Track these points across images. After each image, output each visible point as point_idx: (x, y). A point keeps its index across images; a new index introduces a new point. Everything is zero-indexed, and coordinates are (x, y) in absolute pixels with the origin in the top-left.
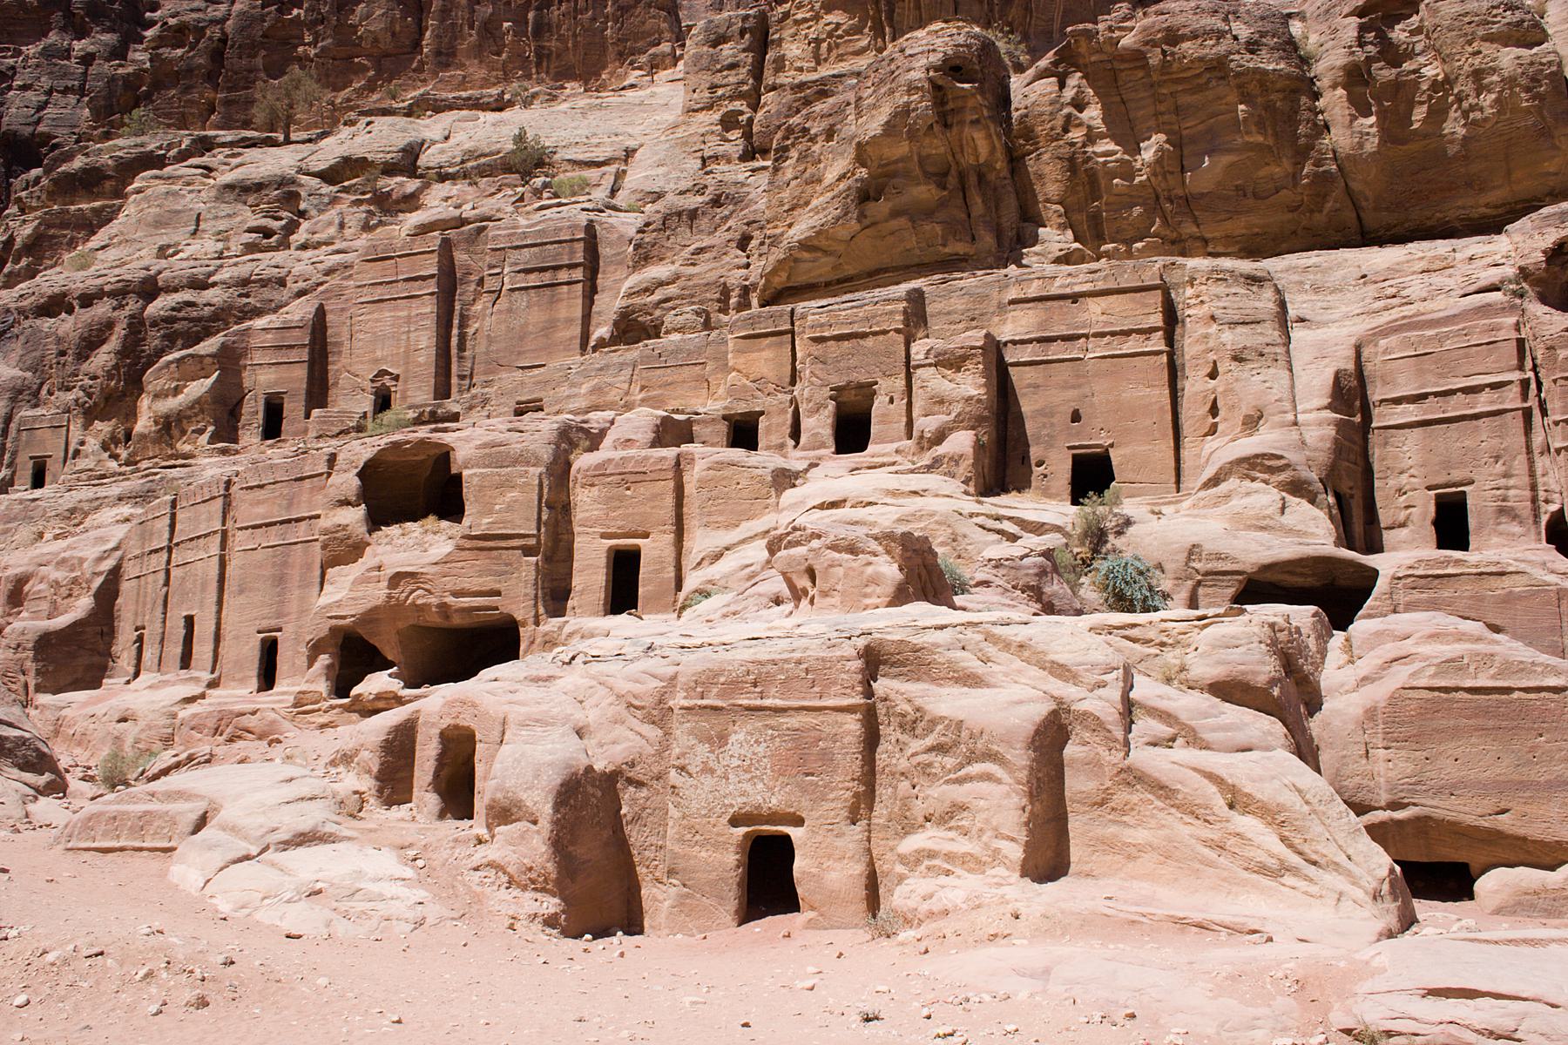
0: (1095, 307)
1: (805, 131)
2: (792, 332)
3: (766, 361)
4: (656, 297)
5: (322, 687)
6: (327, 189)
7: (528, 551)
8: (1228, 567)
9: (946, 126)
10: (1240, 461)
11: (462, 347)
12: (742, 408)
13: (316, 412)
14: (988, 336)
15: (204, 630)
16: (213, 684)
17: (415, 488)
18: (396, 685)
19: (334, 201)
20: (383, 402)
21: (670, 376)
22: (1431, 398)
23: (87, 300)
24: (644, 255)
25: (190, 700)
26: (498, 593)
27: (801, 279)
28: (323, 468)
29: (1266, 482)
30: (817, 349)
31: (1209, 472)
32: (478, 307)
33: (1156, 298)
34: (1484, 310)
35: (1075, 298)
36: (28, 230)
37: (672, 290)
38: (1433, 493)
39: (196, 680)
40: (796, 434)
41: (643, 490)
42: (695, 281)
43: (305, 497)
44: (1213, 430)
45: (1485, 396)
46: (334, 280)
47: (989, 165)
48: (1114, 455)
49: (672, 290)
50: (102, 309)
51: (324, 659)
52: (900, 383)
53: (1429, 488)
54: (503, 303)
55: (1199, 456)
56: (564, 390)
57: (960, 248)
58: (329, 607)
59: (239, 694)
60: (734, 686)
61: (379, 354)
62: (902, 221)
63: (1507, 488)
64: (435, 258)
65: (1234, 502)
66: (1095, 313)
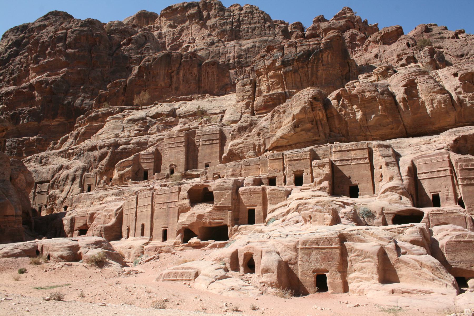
0: (353, 153)
1: (278, 111)
2: (283, 159)
3: (277, 165)
4: (238, 147)
5: (180, 241)
6: (153, 120)
7: (229, 210)
8: (391, 212)
9: (313, 111)
10: (390, 188)
12: (272, 175)
13: (156, 174)
14: (330, 160)
15: (147, 228)
16: (151, 240)
17: (201, 195)
18: (199, 240)
19: (155, 123)
20: (172, 172)
21: (250, 167)
23: (101, 147)
25: (147, 243)
26: (223, 219)
27: (279, 145)
28: (177, 190)
29: (396, 192)
31: (382, 190)
33: (366, 151)
34: (440, 154)
35: (348, 151)
36: (83, 130)
37: (242, 145)
39: (146, 239)
40: (285, 182)
41: (256, 196)
43: (173, 197)
45: (442, 172)
46: (159, 143)
47: (322, 119)
49: (242, 145)
50: (104, 150)
51: (180, 235)
52: (309, 170)
55: (379, 186)
56: (225, 170)
57: (317, 138)
58: (182, 222)
59: (157, 242)
60: (312, 243)
61: (171, 160)
62: (303, 132)
64: (184, 138)
65: (389, 197)
66: (353, 154)
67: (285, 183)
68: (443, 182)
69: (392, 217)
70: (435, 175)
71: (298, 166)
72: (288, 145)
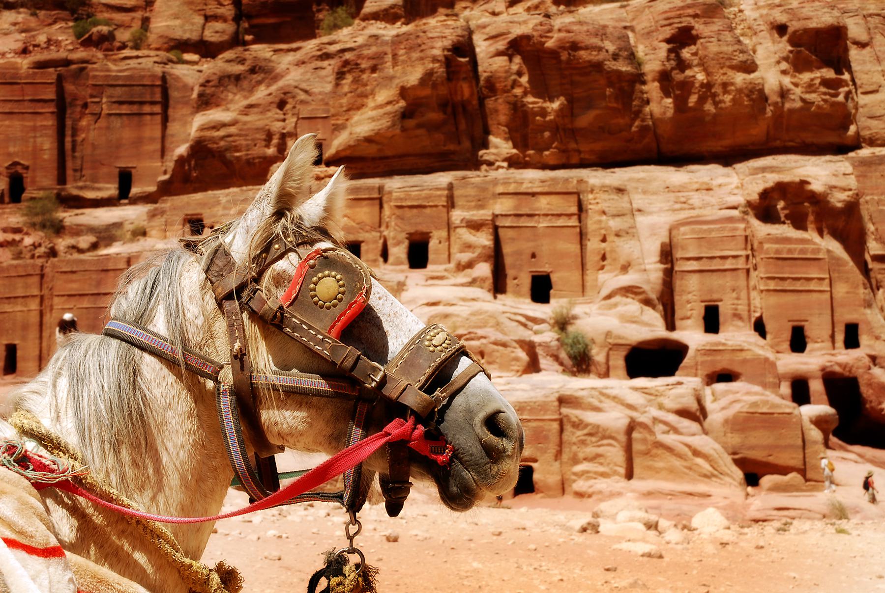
11: (74, 149)
22: (704, 260)
24: (205, 102)
29: (633, 299)
30: (399, 212)
31: (605, 292)
32: (84, 123)
33: (574, 199)
34: (730, 219)
35: (533, 194)
37: (233, 130)
38: (703, 304)
40: (385, 255)
42: (249, 126)
44: (602, 268)
45: (729, 261)
48: (554, 278)
49: (233, 130)
52: (444, 234)
53: (702, 302)
54: (102, 123)
62: (420, 132)
63: (738, 305)
66: (543, 204)
67: (386, 260)
68: (728, 281)
69: (624, 353)
70: (716, 265)
71: (418, 220)
72: (381, 158)
